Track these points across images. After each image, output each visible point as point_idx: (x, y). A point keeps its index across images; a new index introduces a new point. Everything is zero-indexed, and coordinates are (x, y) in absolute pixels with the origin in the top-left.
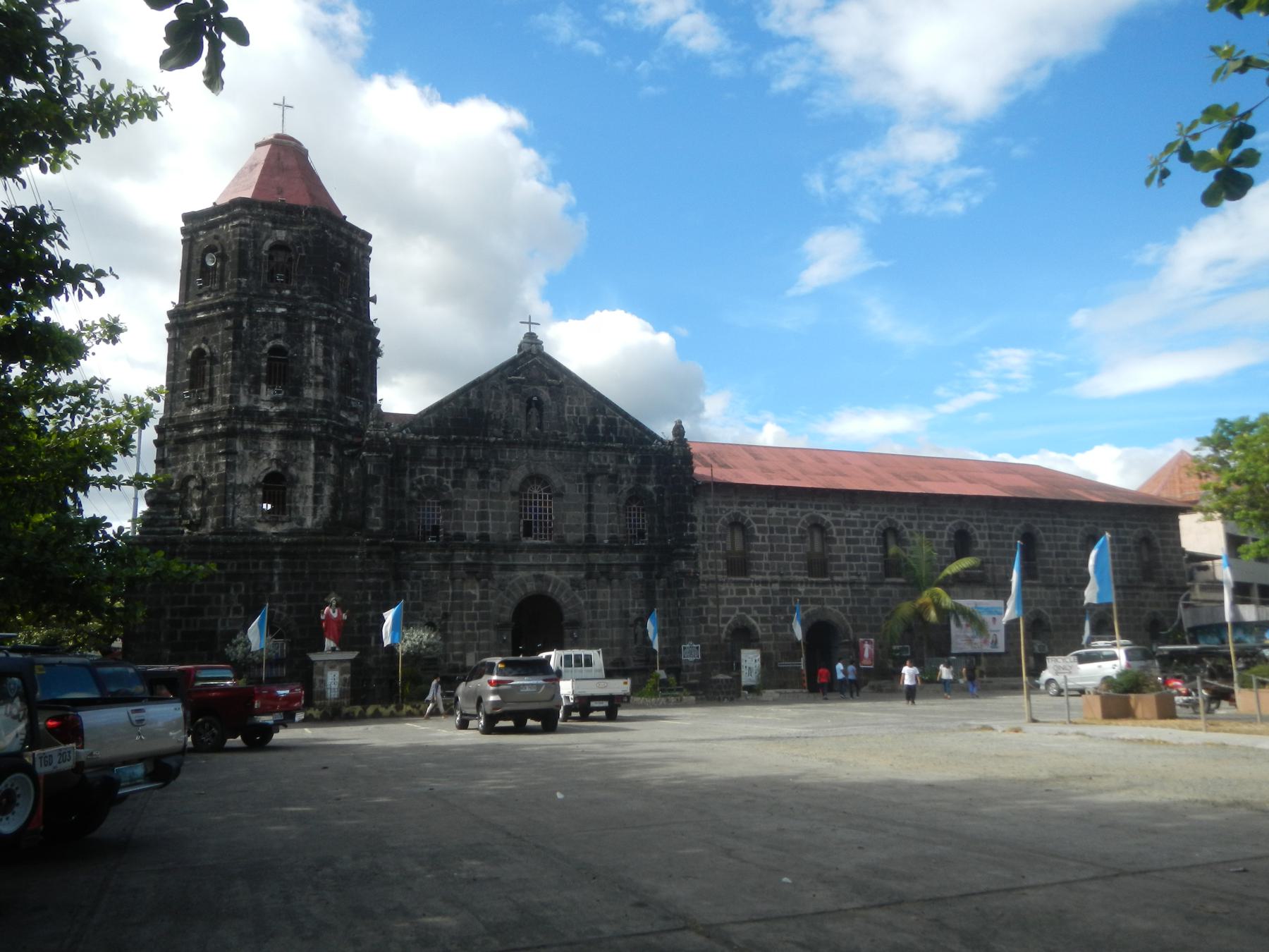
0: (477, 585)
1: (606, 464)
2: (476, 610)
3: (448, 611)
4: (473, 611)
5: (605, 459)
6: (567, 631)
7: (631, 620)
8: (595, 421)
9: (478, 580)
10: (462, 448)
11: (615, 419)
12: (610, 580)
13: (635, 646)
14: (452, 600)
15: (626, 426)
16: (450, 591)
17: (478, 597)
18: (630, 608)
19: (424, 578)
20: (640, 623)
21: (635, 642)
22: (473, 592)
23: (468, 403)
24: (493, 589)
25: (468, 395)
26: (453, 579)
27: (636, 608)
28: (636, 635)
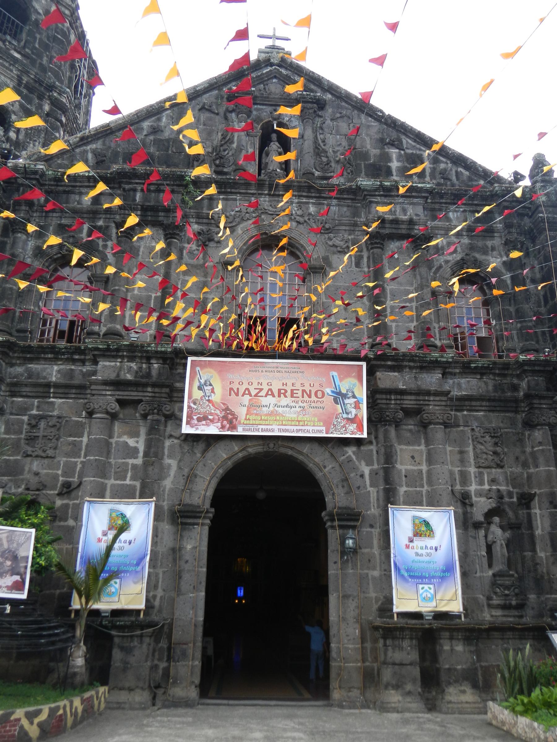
0: (143, 431)
1: (405, 218)
2: (133, 478)
3: (76, 479)
4: (128, 482)
5: (404, 211)
6: (333, 536)
7: (478, 515)
8: (387, 158)
9: (144, 416)
10: (135, 190)
11: (422, 155)
12: (424, 425)
13: (490, 573)
14: (85, 457)
15: (442, 166)
16: (85, 440)
17: (141, 454)
18: (473, 488)
19: (34, 412)
20: (496, 519)
21: (490, 566)
22: (131, 442)
23: (155, 130)
24: (171, 436)
25: (159, 120)
26: (90, 414)
27: (486, 487)
28: (489, 548)
